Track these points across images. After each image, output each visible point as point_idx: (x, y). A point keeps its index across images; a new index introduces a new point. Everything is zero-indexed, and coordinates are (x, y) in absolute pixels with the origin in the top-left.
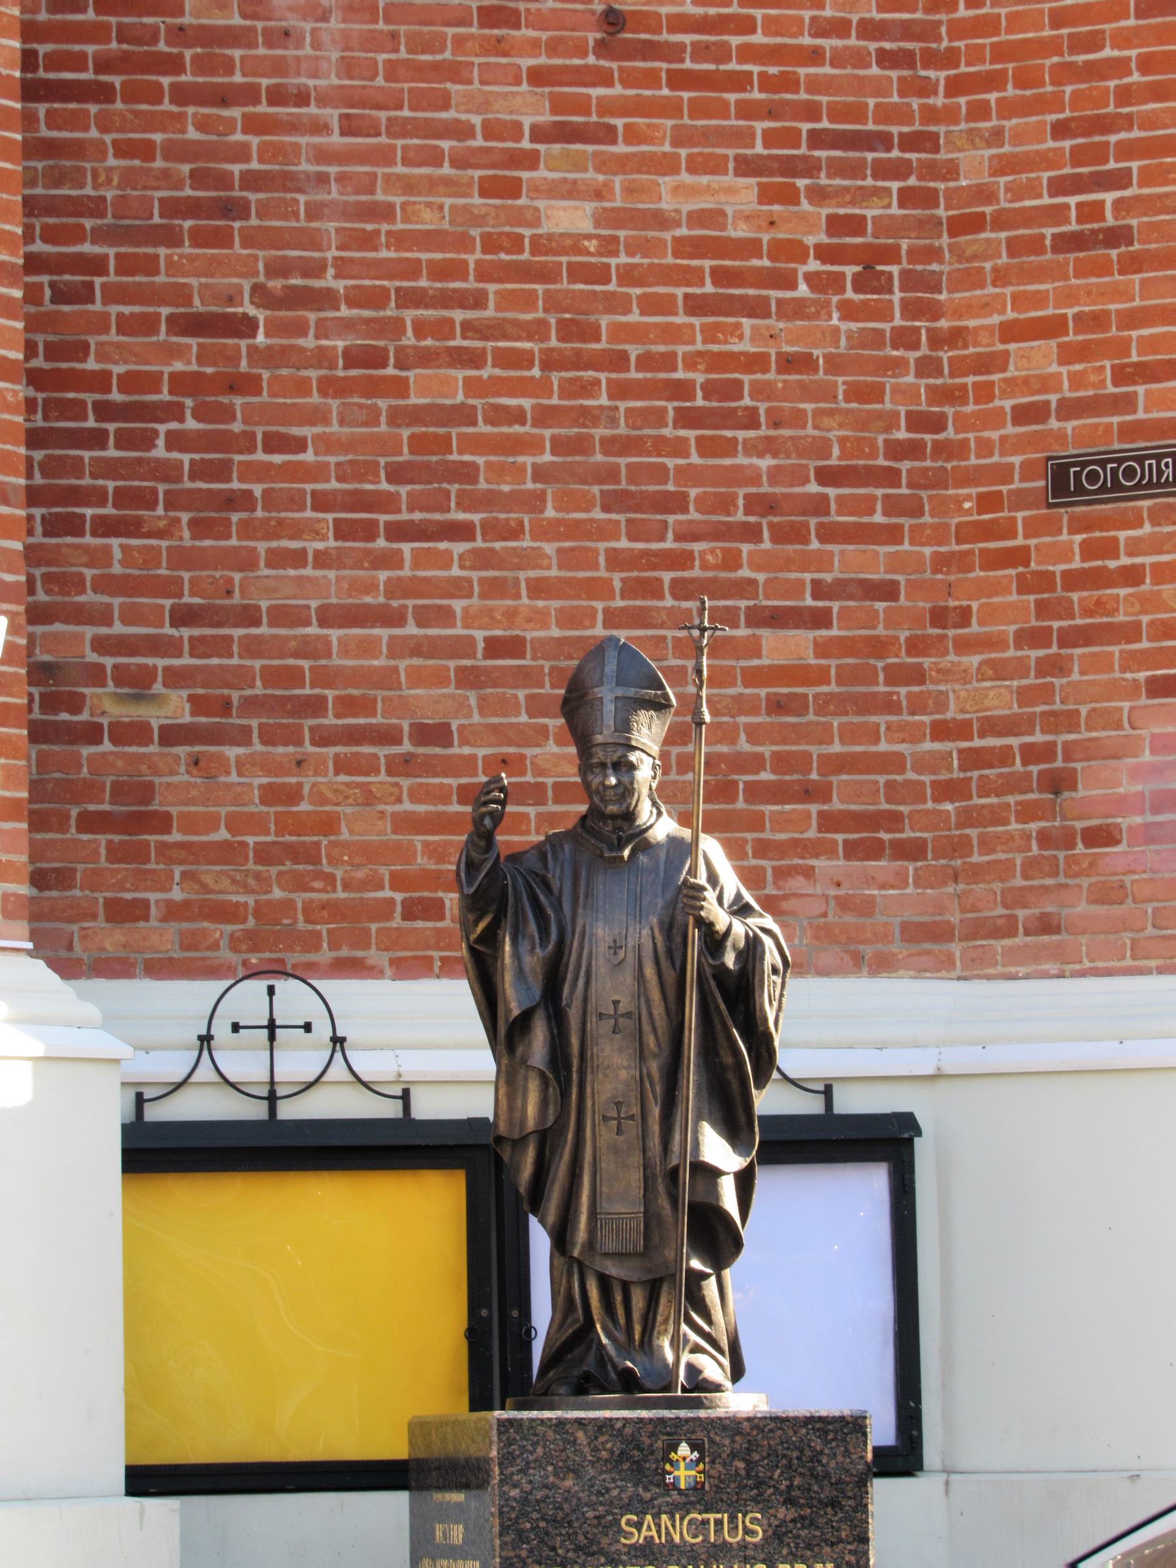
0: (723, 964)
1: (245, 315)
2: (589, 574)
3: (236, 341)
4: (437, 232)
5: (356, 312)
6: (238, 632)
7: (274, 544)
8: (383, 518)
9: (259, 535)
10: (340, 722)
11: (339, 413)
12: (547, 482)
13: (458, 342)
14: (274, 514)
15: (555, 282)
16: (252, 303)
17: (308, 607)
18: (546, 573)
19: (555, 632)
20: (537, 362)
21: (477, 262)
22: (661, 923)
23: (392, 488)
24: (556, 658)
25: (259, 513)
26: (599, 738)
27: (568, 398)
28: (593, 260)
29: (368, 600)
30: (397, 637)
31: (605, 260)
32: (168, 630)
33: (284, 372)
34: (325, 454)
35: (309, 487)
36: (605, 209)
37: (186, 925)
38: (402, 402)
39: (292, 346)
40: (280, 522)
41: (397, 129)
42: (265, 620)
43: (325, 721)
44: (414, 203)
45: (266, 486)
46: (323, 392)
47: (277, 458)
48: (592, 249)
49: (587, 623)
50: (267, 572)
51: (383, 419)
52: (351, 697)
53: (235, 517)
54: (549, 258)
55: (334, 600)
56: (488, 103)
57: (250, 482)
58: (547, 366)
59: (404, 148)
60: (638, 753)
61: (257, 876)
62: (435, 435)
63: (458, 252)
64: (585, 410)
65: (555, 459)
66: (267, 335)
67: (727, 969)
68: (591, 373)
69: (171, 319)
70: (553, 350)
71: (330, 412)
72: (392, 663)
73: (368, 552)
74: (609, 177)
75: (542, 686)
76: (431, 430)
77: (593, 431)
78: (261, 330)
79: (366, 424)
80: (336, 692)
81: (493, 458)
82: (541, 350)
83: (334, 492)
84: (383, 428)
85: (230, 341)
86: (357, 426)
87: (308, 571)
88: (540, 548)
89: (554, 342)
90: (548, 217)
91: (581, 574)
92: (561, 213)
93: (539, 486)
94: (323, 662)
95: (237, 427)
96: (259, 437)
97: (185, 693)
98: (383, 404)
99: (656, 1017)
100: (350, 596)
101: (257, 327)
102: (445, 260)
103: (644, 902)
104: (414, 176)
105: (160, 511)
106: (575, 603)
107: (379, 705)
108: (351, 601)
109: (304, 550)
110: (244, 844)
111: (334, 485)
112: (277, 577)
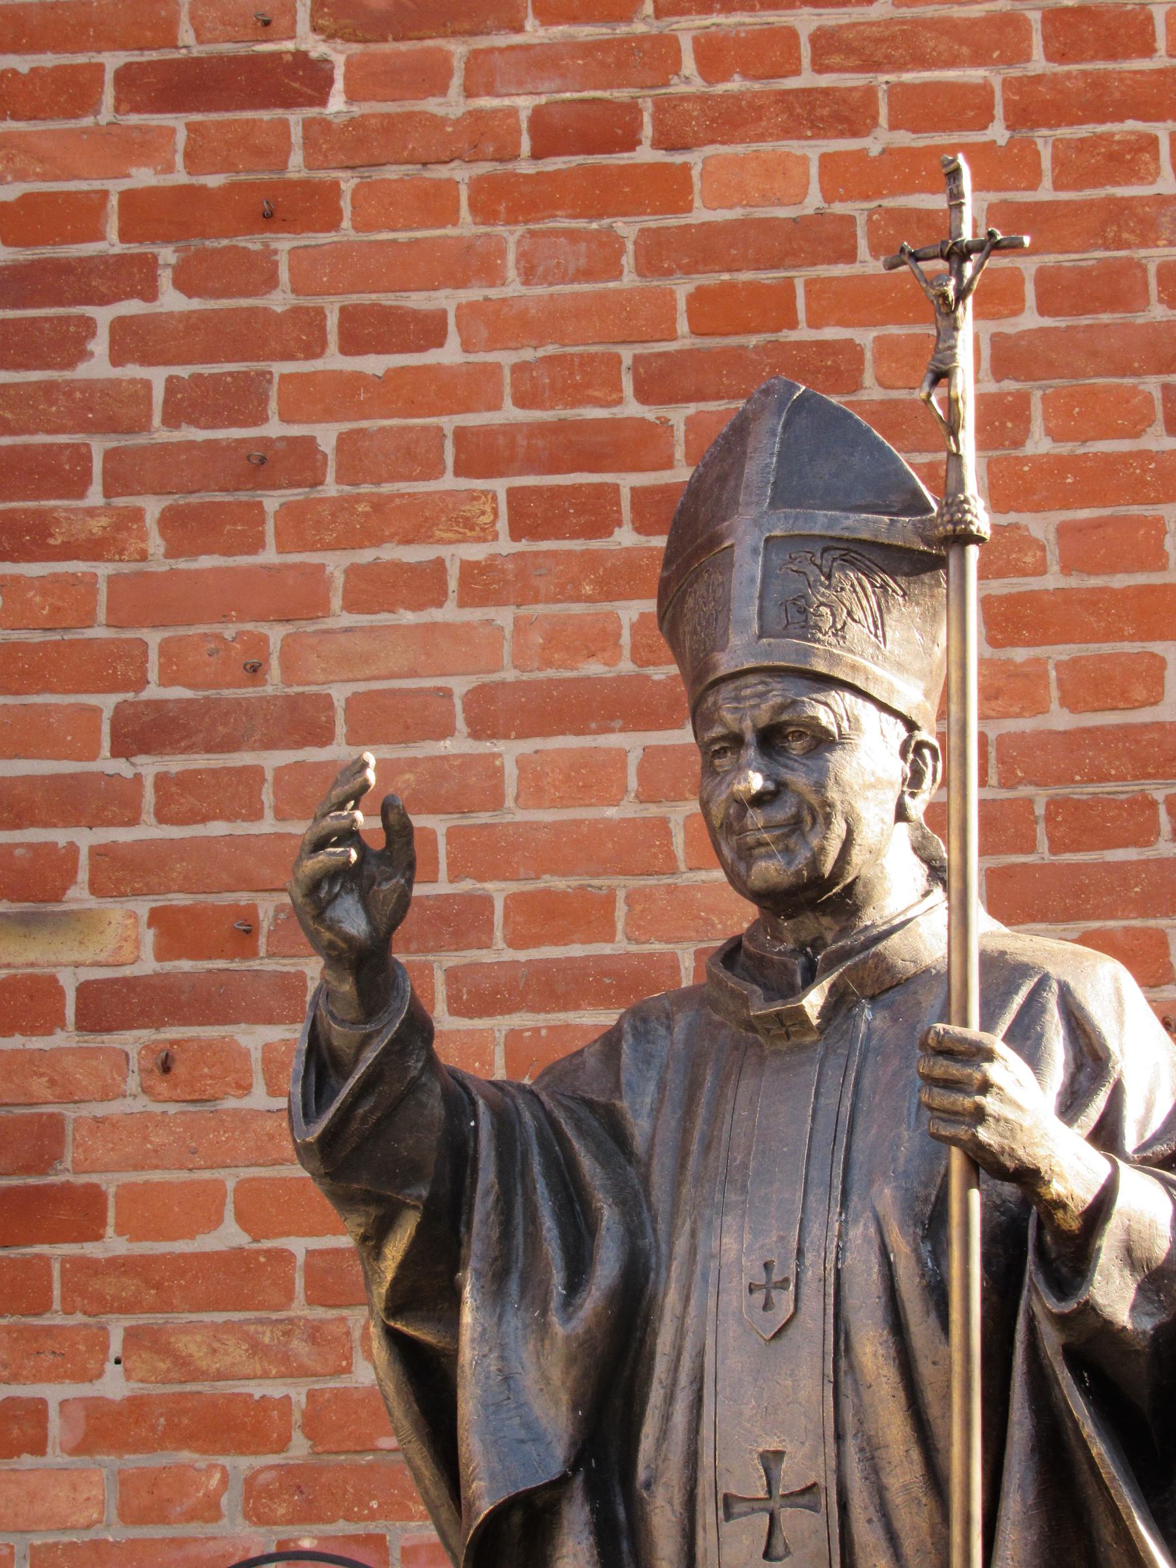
0: (1089, 1309)
1: (301, 57)
2: (1141, 579)
3: (278, 113)
5: (559, 31)
6: (273, 760)
7: (366, 556)
8: (628, 482)
9: (328, 538)
10: (523, 956)
11: (522, 256)
12: (1030, 378)
13: (807, 79)
14: (366, 489)
16: (315, 29)
17: (447, 693)
18: (1034, 584)
19: (1060, 719)
20: (999, 111)
22: (909, 1202)
23: (649, 413)
24: (1059, 780)
25: (331, 488)
26: (725, 663)
27: (1077, 186)
29: (594, 668)
30: (664, 749)
32: (107, 764)
33: (392, 173)
34: (490, 349)
35: (448, 423)
37: (135, 1461)
38: (672, 221)
39: (410, 116)
40: (379, 505)
42: (341, 729)
43: (486, 956)
45: (347, 426)
46: (484, 211)
47: (374, 364)
49: (1139, 693)
50: (348, 620)
51: (628, 261)
52: (548, 892)
53: (272, 501)
55: (510, 675)
57: (309, 421)
58: (1020, 117)
60: (842, 701)
61: (315, 1333)
62: (754, 288)
64: (1119, 210)
65: (1048, 322)
66: (352, 96)
67: (1107, 1328)
68: (1132, 125)
69: (124, 76)
70: (1038, 79)
71: (502, 253)
72: (653, 810)
73: (591, 560)
75: (1030, 847)
76: (745, 276)
77: (1143, 253)
78: (339, 85)
79: (587, 274)
80: (513, 887)
81: (893, 330)
82: (1007, 84)
83: (510, 430)
84: (629, 280)
85: (265, 115)
86: (563, 281)
87: (449, 613)
88: (1015, 527)
89: (1039, 63)
91: (1120, 581)
93: (1010, 385)
94: (484, 818)
95: (279, 301)
96: (332, 321)
97: (143, 907)
98: (627, 228)
99: (896, 1498)
100: (548, 663)
101: (330, 81)
103: (859, 1144)
105: (95, 496)
106: (1106, 648)
107: (621, 911)
108: (551, 673)
109: (439, 564)
110: (283, 1257)
111: (510, 413)
112: (372, 630)
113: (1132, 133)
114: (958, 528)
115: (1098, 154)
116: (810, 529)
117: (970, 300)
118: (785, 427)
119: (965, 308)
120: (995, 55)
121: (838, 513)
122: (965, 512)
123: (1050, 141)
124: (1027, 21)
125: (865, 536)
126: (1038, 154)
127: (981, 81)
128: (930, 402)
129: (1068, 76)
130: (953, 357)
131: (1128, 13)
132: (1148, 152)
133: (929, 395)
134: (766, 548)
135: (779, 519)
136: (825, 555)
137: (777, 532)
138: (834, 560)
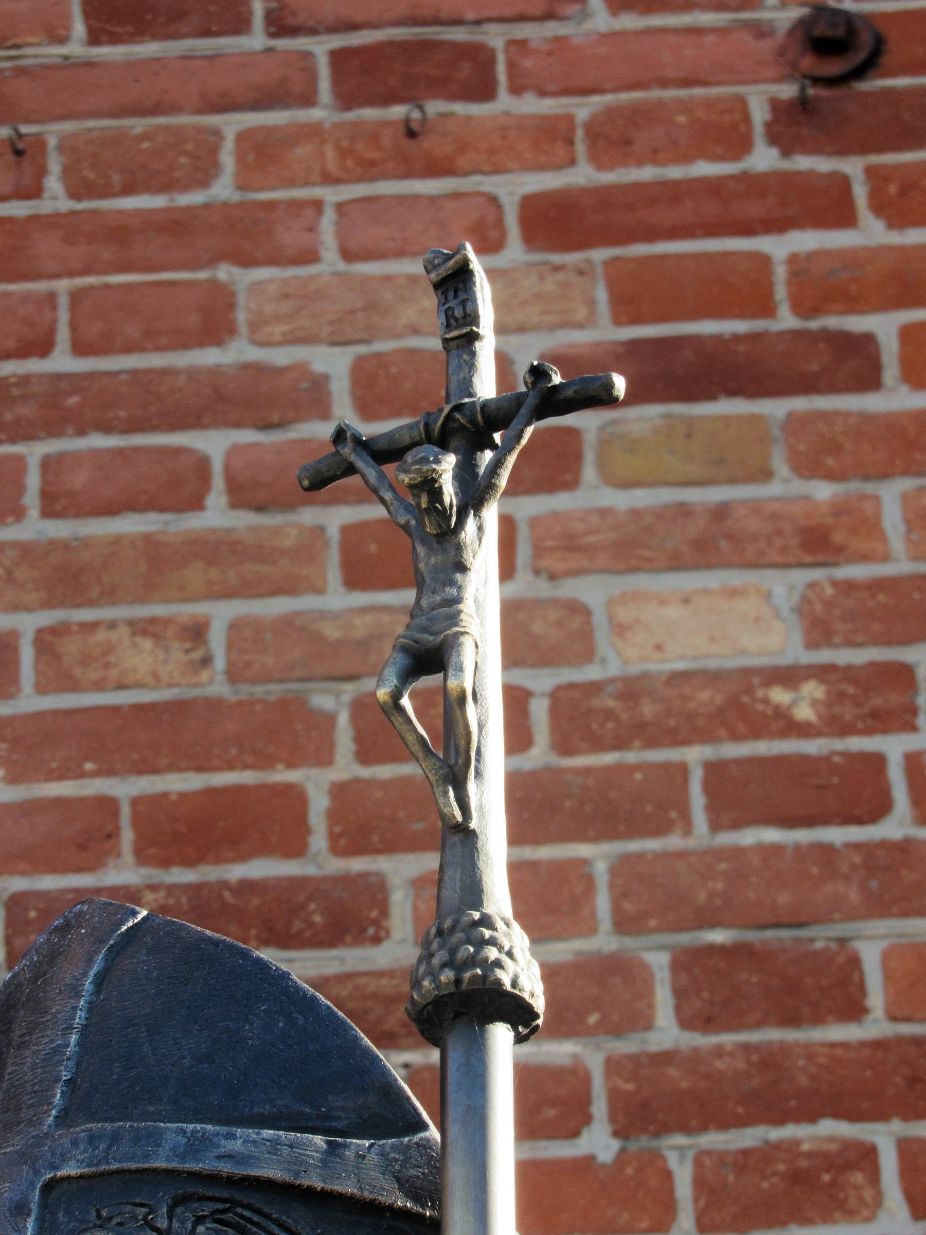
4: (180, 707)
15: (660, 829)
20: (600, 1107)
21: (339, 791)
28: (811, 747)
31: (857, 744)
36: (847, 587)
41: (24, 410)
44: (92, 626)
48: (804, 713)
54: (631, 757)
56: (371, 306)
59: (47, 464)
63: (264, 761)
70: (666, 1057)
74: (854, 486)
82: (612, 1066)
90: (620, 629)
92: (674, 612)
102: (210, 792)
104: (86, 543)
113: (831, 1139)
114: (467, 975)
115: (774, 1174)
116: (146, 1157)
117: (491, 513)
118: (99, 982)
119: (480, 528)
120: (593, 1019)
121: (209, 1127)
122: (483, 943)
123: (690, 1155)
124: (645, 967)
125: (272, 1172)
126: (667, 1176)
127: (567, 1061)
128: (401, 710)
129: (719, 1052)
130: (454, 619)
131: (817, 954)
132: (861, 1170)
133: (396, 696)
134: (44, 1205)
135: (75, 1143)
136: (179, 1210)
137: (71, 1170)
138: (199, 1220)
